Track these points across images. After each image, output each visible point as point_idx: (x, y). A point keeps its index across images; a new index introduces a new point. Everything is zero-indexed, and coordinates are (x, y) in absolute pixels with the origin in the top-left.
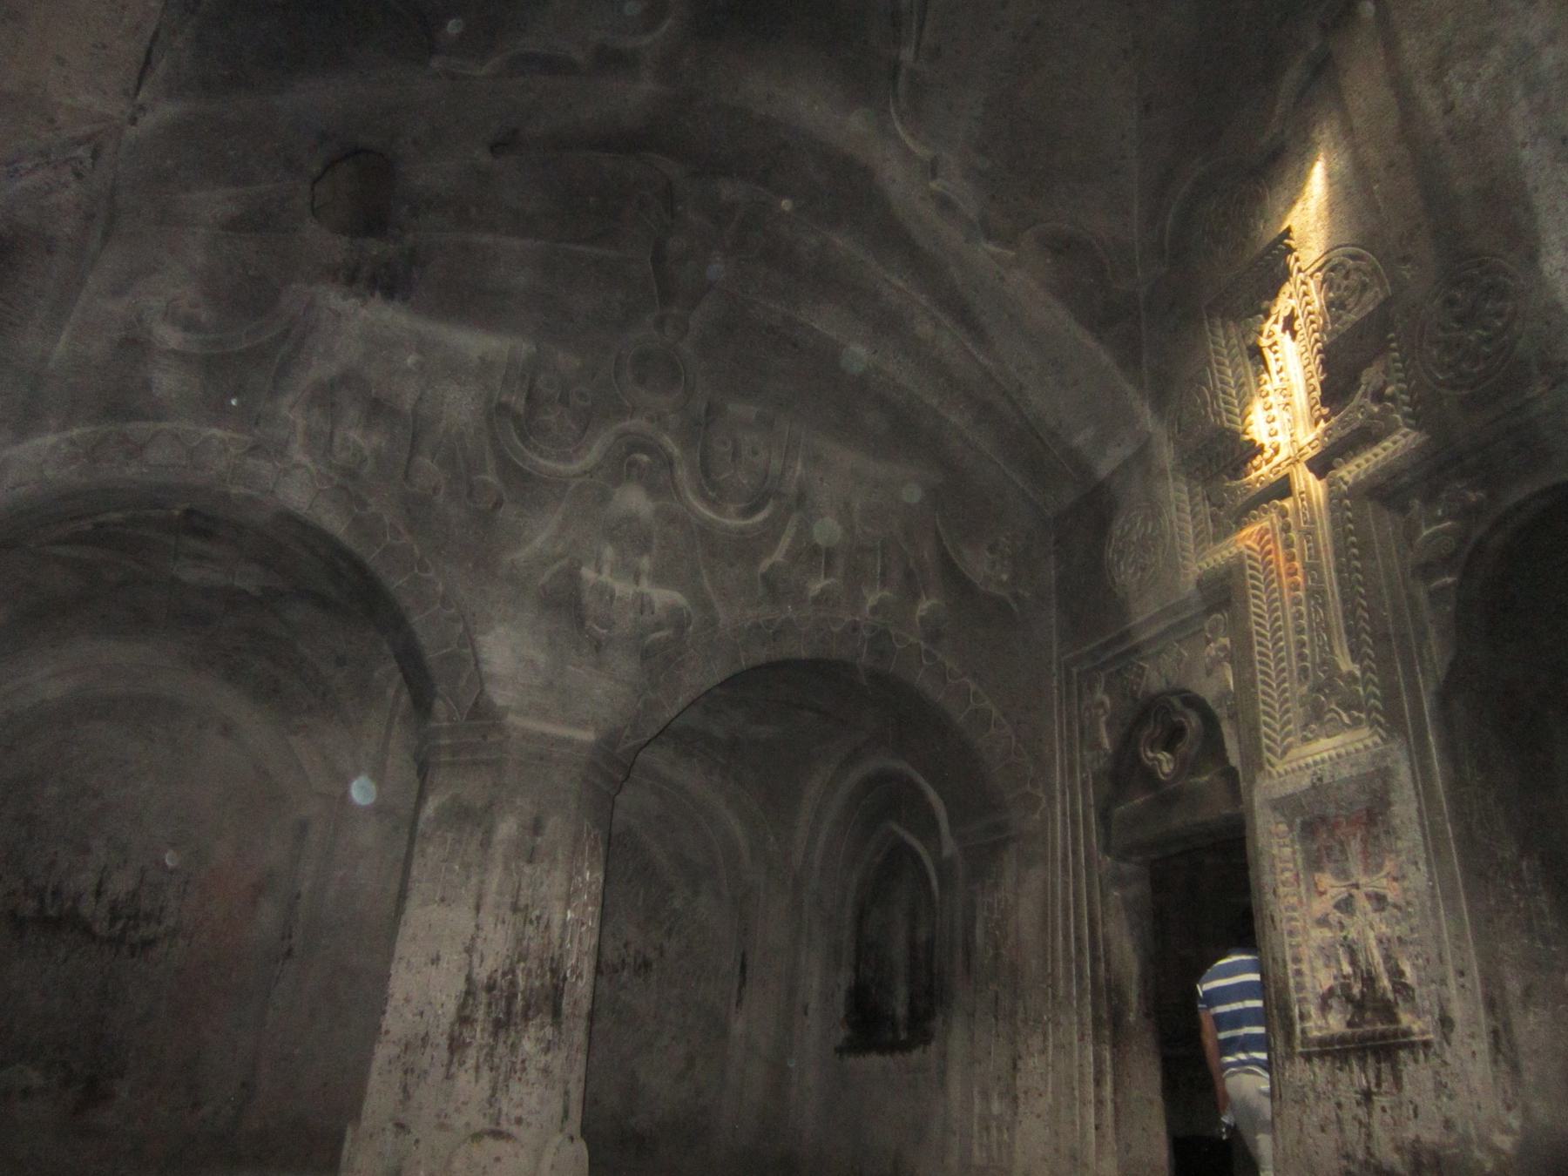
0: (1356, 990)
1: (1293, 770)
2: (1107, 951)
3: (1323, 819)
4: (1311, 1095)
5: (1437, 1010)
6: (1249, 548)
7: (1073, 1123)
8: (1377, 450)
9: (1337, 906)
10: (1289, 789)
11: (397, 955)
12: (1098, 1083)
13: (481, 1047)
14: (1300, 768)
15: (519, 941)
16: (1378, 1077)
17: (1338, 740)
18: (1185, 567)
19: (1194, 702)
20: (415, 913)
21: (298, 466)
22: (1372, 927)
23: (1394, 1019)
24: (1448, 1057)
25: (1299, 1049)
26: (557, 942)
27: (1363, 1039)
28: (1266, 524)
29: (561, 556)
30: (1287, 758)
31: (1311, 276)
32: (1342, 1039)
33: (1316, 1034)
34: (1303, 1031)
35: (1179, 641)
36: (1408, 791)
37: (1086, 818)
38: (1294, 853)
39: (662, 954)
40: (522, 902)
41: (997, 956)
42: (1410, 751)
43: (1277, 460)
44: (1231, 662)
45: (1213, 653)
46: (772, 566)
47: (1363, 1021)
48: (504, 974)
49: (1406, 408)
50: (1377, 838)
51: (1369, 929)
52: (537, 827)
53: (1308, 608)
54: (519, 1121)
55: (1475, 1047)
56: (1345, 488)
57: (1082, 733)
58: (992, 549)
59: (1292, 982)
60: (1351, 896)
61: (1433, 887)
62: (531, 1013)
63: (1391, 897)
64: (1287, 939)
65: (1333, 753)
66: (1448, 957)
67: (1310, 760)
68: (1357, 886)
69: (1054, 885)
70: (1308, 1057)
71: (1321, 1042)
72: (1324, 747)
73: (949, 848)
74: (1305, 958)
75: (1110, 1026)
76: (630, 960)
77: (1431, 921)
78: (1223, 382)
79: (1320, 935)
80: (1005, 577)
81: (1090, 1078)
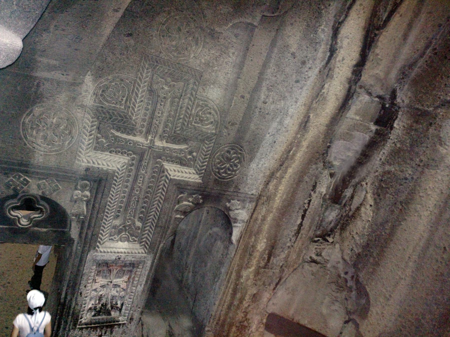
1: (108, 252)
6: (119, 169)
10: (105, 258)
14: (111, 252)
18: (79, 156)
24: (129, 327)
30: (104, 245)
31: (199, 99)
36: (148, 268)
45: (80, 196)
47: (99, 315)
49: (198, 167)
60: (108, 284)
67: (116, 251)
68: (111, 282)
78: (137, 94)
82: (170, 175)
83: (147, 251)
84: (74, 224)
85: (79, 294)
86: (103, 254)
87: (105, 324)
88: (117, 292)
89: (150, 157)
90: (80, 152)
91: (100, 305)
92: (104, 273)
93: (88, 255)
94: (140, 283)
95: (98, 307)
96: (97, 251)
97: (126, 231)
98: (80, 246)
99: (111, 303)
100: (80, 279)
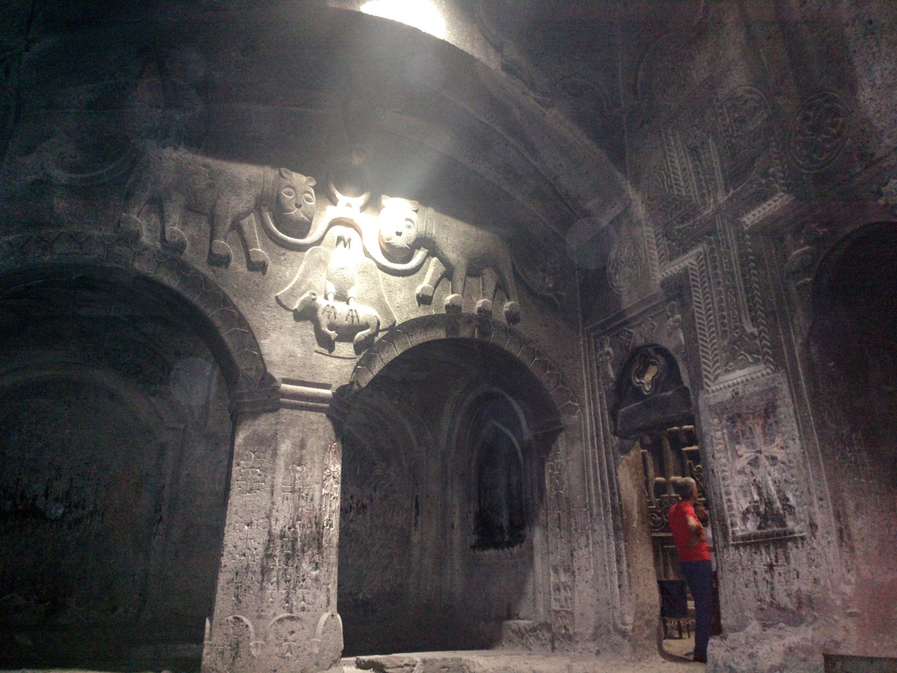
0: (762, 509)
2: (618, 490)
3: (739, 415)
4: (740, 568)
5: (808, 520)
6: (691, 263)
7: (606, 584)
8: (765, 205)
9: (749, 463)
11: (227, 523)
12: (618, 561)
13: (279, 570)
14: (725, 387)
15: (296, 509)
16: (776, 557)
17: (745, 371)
18: (654, 275)
19: (662, 351)
20: (236, 500)
21: (146, 249)
22: (770, 475)
23: (784, 525)
25: (731, 542)
26: (317, 507)
27: (767, 536)
28: (700, 249)
29: (304, 292)
30: (717, 382)
32: (756, 536)
33: (740, 534)
34: (733, 533)
35: (652, 317)
36: (788, 400)
37: (603, 415)
38: (723, 434)
39: (372, 500)
40: (297, 487)
41: (558, 496)
42: (788, 378)
43: (706, 212)
44: (683, 329)
45: (672, 323)
46: (423, 289)
47: (767, 526)
48: (289, 529)
49: (782, 181)
50: (771, 425)
51: (769, 476)
52: (302, 445)
53: (726, 296)
54: (303, 609)
55: (830, 539)
56: (746, 228)
57: (598, 367)
58: (543, 270)
59: (726, 506)
60: (757, 457)
61: (804, 453)
62: (306, 548)
63: (780, 457)
64: (721, 482)
65: (744, 379)
66: (813, 490)
67: (730, 383)
68: (760, 452)
69: (587, 454)
70: (737, 547)
71: (743, 538)
72: (739, 375)
73: (527, 435)
74: (733, 492)
75: (621, 529)
76: (354, 506)
77: (804, 471)
79: (740, 479)
80: (551, 285)
81: (615, 559)
82: (747, 225)
84: (681, 366)
89: (724, 224)
90: (653, 270)
97: (737, 350)
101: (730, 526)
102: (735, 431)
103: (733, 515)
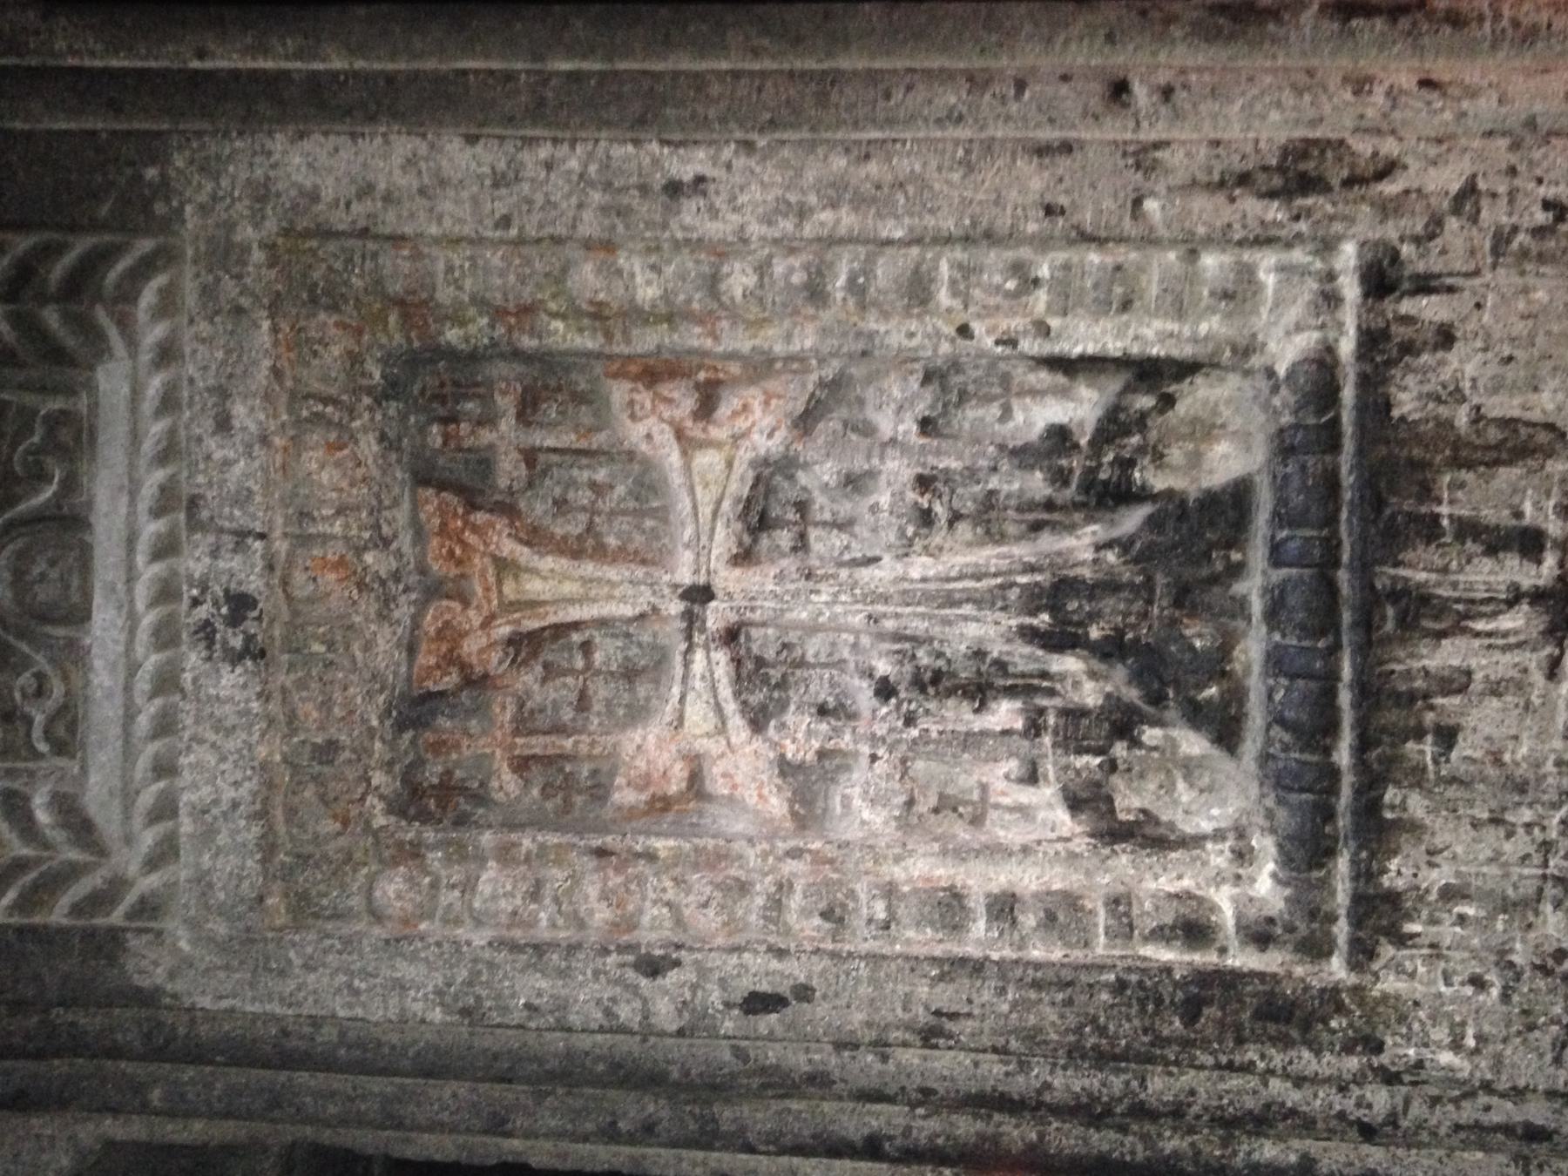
0: (1082, 681)
3: (416, 710)
14: (165, 726)
24: (1447, 179)
25: (1337, 969)
33: (1266, 886)
34: (1260, 935)
38: (506, 855)
47: (1217, 664)
60: (731, 636)
64: (863, 940)
68: (700, 594)
70: (1380, 916)
71: (1307, 853)
77: (905, 165)
83: (145, 245)
85: (769, 1021)
86: (186, 826)
87: (1343, 576)
88: (854, 483)
91: (1069, 664)
92: (583, 702)
93: (206, 1002)
94: (645, 209)
95: (1090, 695)
96: (148, 908)
98: (139, 1088)
99: (1042, 517)
100: (558, 1042)
101: (1205, 958)
102: (506, 783)
103: (1118, 903)
